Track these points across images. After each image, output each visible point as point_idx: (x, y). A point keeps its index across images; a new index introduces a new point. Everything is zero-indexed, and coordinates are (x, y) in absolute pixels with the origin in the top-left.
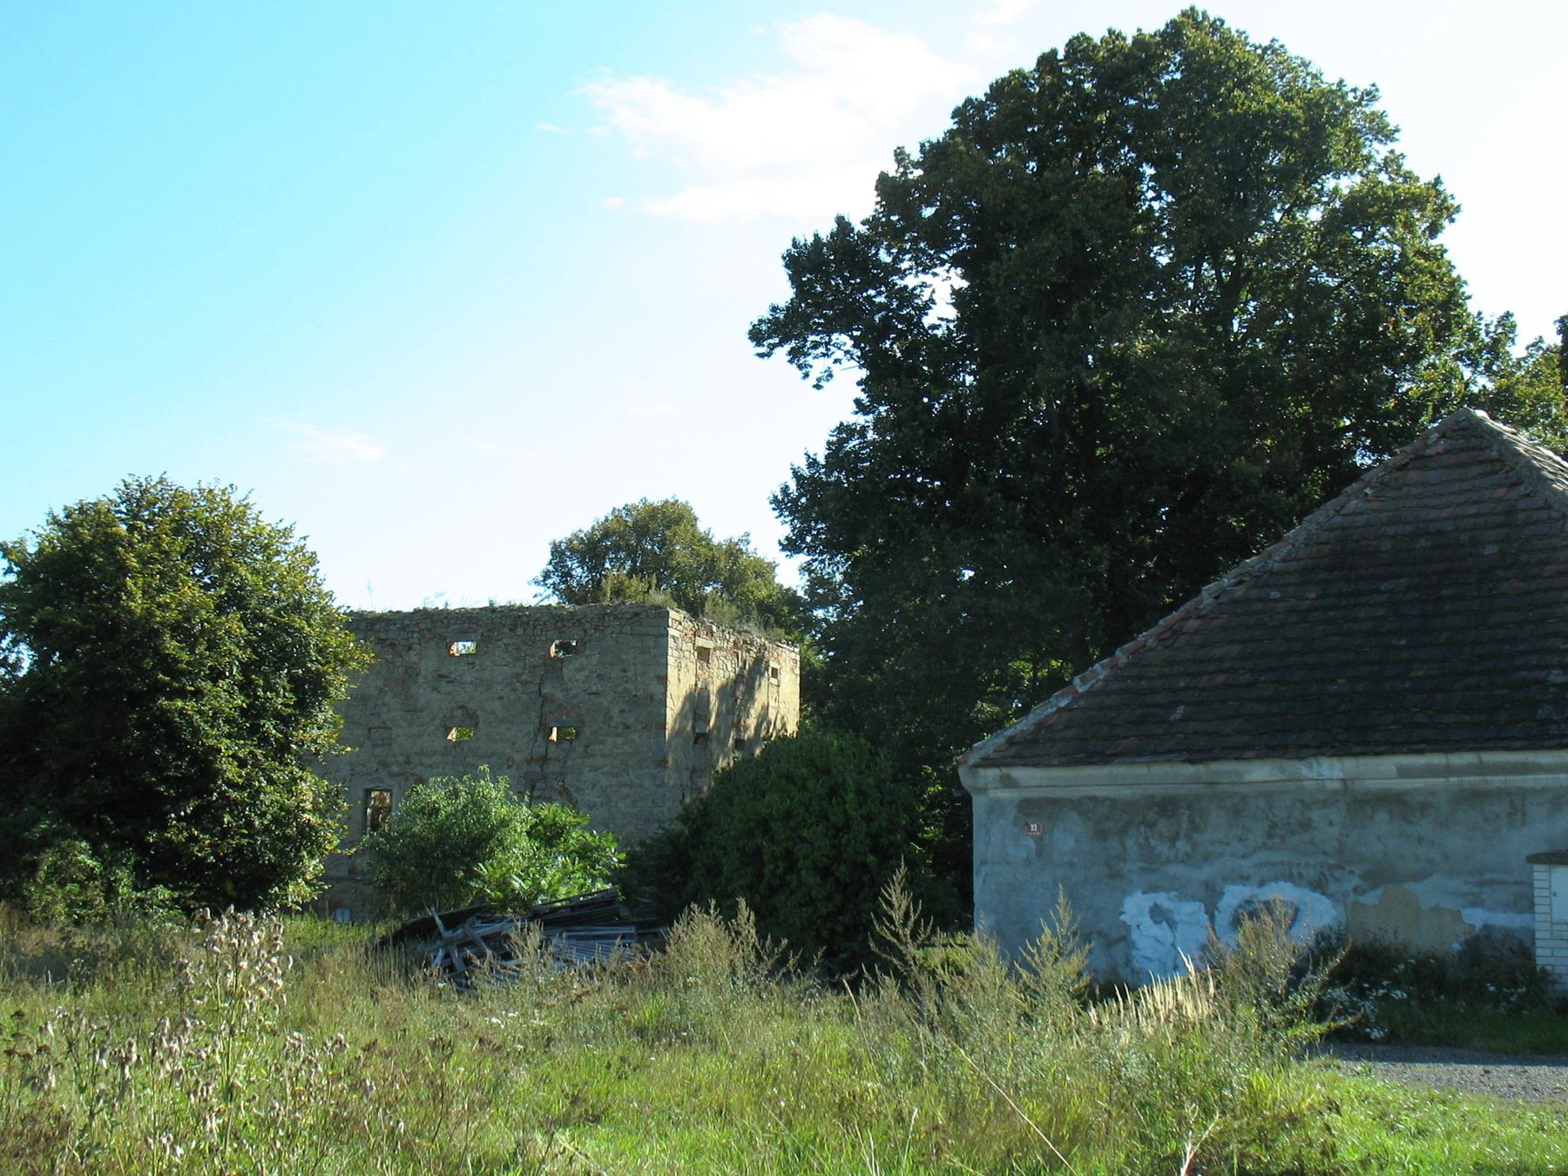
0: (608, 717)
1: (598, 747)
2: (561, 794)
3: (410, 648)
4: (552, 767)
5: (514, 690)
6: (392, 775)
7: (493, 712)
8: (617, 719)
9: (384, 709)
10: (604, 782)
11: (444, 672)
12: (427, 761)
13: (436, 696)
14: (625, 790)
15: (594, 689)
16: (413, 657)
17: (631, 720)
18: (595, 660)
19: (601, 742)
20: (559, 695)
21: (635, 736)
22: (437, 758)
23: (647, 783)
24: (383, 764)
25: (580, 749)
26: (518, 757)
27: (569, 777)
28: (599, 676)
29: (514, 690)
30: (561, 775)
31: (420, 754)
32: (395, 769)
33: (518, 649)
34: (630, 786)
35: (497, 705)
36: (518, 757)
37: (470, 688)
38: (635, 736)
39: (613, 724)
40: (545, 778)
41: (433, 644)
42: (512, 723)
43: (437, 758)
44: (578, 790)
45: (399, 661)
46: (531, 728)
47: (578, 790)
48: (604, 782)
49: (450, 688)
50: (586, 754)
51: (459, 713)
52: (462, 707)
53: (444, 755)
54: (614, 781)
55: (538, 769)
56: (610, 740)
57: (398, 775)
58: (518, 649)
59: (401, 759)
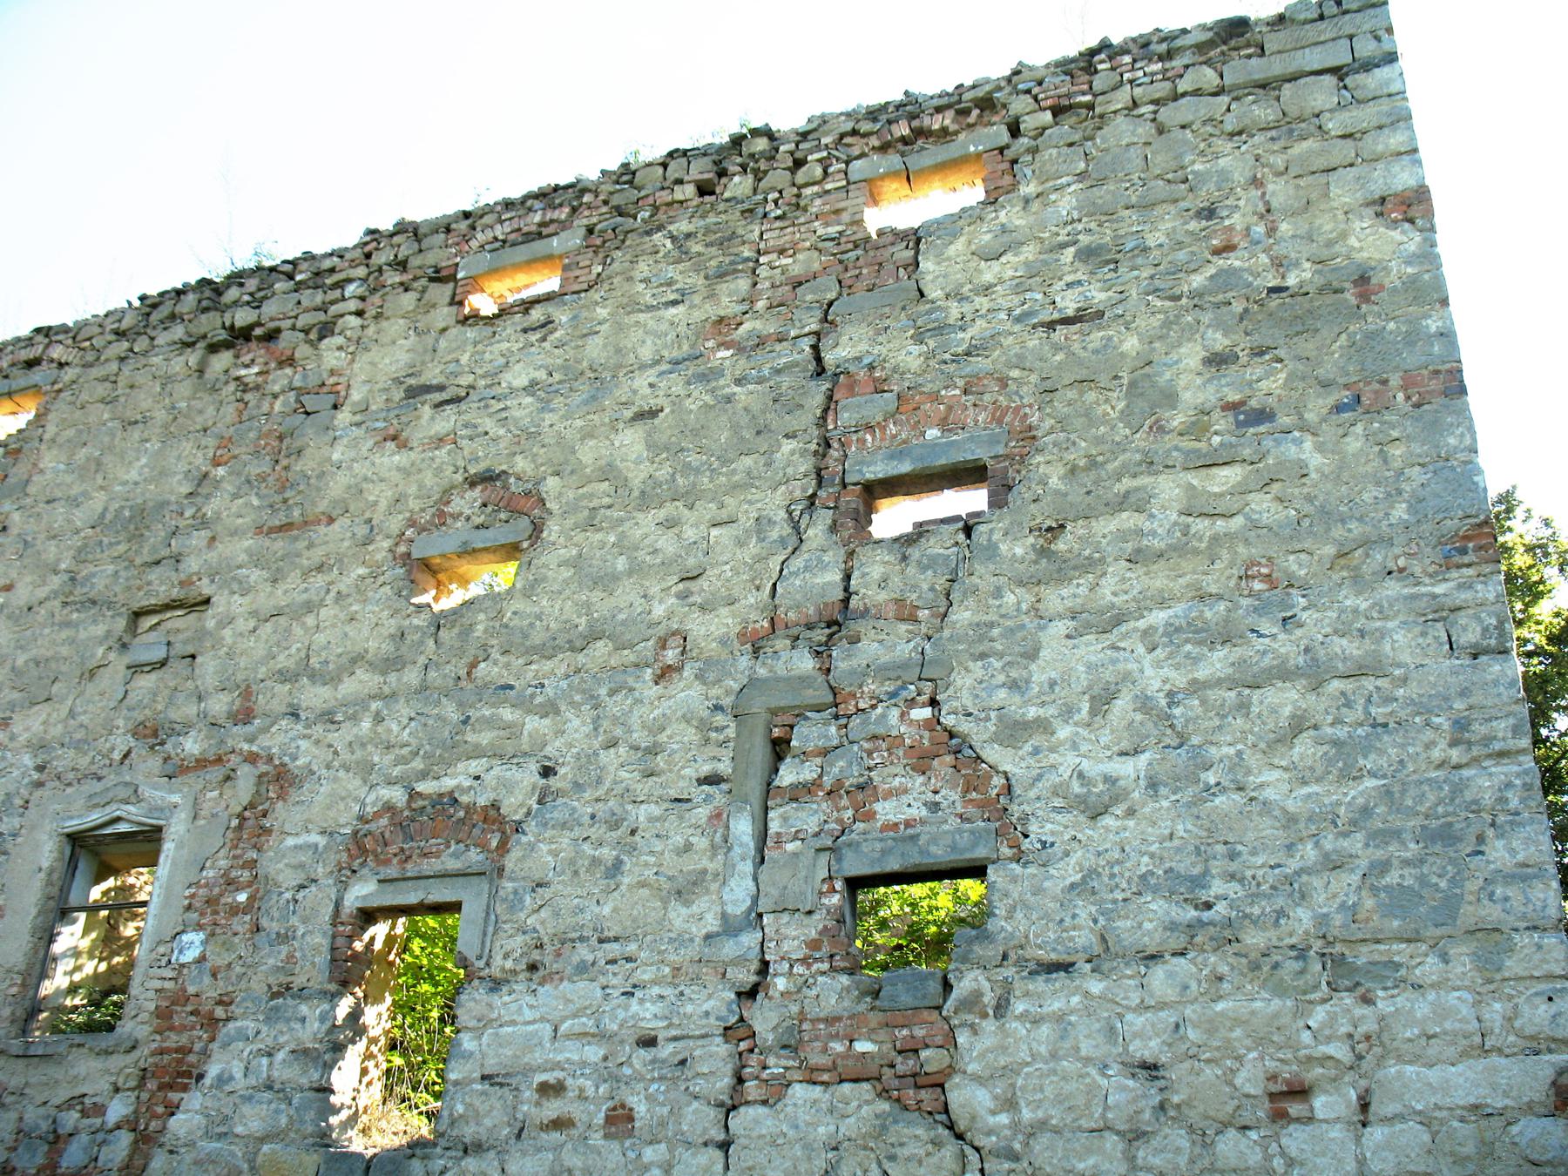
0: (1148, 395)
1: (1106, 526)
2: (921, 762)
3: (326, 330)
4: (878, 647)
6: (176, 771)
7: (608, 473)
8: (1195, 390)
9: (199, 538)
10: (1155, 675)
11: (432, 375)
12: (314, 696)
14: (1285, 699)
15: (1069, 304)
17: (1270, 384)
18: (1066, 204)
19: (1122, 503)
20: (908, 356)
21: (1307, 451)
23: (1401, 643)
25: (1020, 549)
28: (1087, 255)
30: (926, 681)
31: (285, 676)
32: (192, 745)
34: (1315, 673)
35: (631, 440)
36: (711, 629)
37: (523, 409)
38: (1307, 451)
39: (1177, 420)
40: (836, 704)
42: (690, 498)
44: (1013, 731)
45: (280, 379)
46: (774, 503)
47: (1013, 731)
48: (1155, 675)
49: (446, 421)
51: (467, 503)
52: (487, 478)
54: (1217, 662)
55: (805, 663)
56: (1168, 489)
57: (202, 763)
59: (219, 705)
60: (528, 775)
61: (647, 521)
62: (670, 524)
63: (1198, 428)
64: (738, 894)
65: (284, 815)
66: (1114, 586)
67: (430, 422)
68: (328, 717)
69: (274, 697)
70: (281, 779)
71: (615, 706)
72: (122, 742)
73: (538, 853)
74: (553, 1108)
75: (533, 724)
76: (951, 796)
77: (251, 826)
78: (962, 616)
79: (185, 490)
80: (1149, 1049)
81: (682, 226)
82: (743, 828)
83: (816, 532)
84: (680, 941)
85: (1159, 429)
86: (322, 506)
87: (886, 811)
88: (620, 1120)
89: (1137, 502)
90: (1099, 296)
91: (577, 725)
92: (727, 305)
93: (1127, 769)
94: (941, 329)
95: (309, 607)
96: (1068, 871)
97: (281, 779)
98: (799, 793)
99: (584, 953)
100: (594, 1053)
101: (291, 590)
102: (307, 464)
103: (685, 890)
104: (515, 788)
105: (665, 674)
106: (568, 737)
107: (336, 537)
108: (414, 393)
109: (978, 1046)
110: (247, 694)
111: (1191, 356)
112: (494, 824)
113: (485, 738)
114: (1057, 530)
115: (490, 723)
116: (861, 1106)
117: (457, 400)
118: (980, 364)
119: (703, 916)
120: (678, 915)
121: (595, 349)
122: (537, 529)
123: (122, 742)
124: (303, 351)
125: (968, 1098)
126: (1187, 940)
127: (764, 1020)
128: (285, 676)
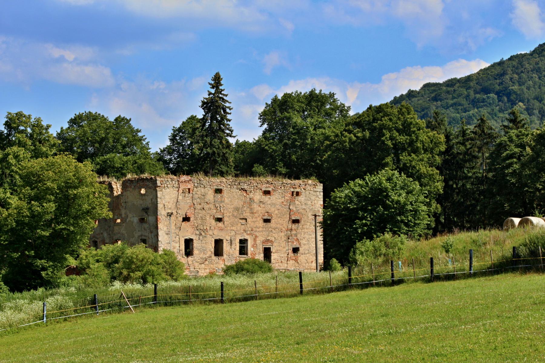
2: (296, 241)
5: (282, 207)
12: (258, 230)
16: (251, 195)
20: (295, 209)
22: (261, 229)
24: (245, 231)
26: (284, 229)
29: (282, 207)
30: (296, 235)
32: (249, 232)
40: (292, 235)
41: (258, 191)
43: (261, 229)
44: (301, 239)
47: (301, 239)
50: (303, 228)
52: (268, 212)
53: (263, 228)
54: (310, 237)
59: (250, 229)
65: (257, 239)
66: (306, 230)
67: (261, 205)
69: (254, 229)
70: (256, 237)
73: (275, 244)
77: (255, 240)
81: (279, 191)
87: (295, 244)
97: (256, 237)
101: (254, 219)
102: (252, 207)
104: (273, 239)
107: (256, 215)
108: (260, 202)
109: (299, 258)
111: (310, 214)
112: (271, 242)
116: (294, 262)
121: (274, 202)
126: (308, 253)
127: (289, 256)
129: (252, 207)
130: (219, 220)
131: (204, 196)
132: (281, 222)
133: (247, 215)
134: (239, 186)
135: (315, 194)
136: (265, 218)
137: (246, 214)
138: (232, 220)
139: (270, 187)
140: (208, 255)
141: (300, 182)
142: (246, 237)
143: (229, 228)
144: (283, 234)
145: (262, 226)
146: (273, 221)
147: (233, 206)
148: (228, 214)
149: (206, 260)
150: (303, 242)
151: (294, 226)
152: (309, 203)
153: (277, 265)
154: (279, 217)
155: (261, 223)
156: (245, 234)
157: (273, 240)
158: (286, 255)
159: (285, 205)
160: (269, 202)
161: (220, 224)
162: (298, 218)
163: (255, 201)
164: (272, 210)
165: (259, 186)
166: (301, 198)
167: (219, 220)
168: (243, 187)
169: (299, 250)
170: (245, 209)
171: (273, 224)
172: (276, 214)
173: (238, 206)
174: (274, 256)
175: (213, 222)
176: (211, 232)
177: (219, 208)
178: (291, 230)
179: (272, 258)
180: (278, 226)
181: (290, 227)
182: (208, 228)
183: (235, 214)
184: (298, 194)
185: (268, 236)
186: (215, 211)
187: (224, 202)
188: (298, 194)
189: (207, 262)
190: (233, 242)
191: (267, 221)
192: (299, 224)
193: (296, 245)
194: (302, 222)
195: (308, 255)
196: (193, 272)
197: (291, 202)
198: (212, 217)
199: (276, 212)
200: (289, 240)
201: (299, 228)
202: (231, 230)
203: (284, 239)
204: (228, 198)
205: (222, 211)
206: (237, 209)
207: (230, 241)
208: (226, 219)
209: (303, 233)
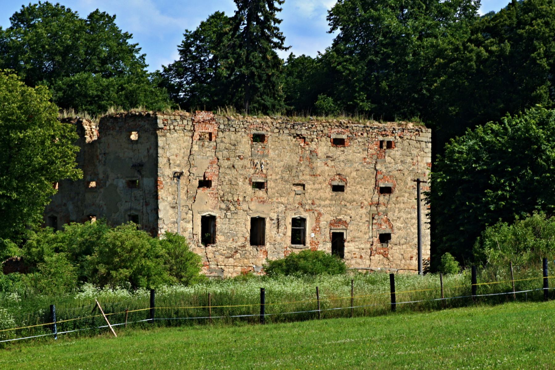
1: (402, 198)
2: (386, 222)
3: (312, 141)
4: (382, 208)
5: (364, 166)
6: (306, 210)
11: (330, 155)
12: (323, 203)
13: (327, 168)
16: (313, 146)
20: (384, 170)
22: (327, 202)
24: (301, 204)
25: (394, 199)
26: (366, 203)
27: (389, 214)
31: (318, 199)
32: (307, 207)
33: (364, 144)
37: (342, 165)
40: (378, 214)
41: (324, 139)
43: (327, 202)
44: (393, 220)
47: (393, 220)
50: (397, 202)
52: (339, 175)
53: (331, 200)
54: (409, 216)
56: (407, 195)
58: (364, 144)
59: (310, 202)
60: (349, 217)
61: (359, 186)
62: (361, 187)
63: (409, 188)
64: (371, 234)
65: (321, 219)
66: (402, 206)
68: (324, 206)
70: (320, 214)
71: (357, 210)
72: (297, 206)
73: (351, 227)
74: (355, 256)
75: (349, 211)
76: (388, 226)
77: (318, 220)
78: (389, 206)
79: (297, 164)
80: (402, 253)
81: (360, 140)
82: (371, 227)
83: (376, 192)
84: (366, 238)
85: (406, 187)
86: (318, 173)
87: (383, 227)
88: (361, 257)
89: (403, 196)
90: (402, 168)
91: (353, 212)
92: (365, 156)
93: (402, 226)
94: (388, 167)
95: (319, 189)
96: (396, 236)
97: (320, 214)
98: (375, 224)
99: (356, 239)
100: (358, 250)
101: (317, 186)
102: (314, 165)
103: (365, 233)
104: (348, 219)
105: (362, 207)
106: (352, 213)
107: (321, 179)
108: (328, 157)
109: (391, 251)
110: (313, 201)
111: (409, 179)
113: (344, 212)
114: (397, 197)
115: (344, 210)
116: (382, 257)
117: (333, 160)
118: (391, 174)
119: (367, 237)
120: (365, 236)
121: (350, 157)
122: (346, 184)
123: (297, 206)
124: (310, 143)
125: (389, 256)
126: (405, 243)
127: (374, 248)
128: (318, 199)
129: (314, 165)
130: (259, 186)
131: (234, 145)
132: (361, 191)
133: (305, 178)
134: (293, 131)
135: (418, 145)
136: (335, 183)
137: (304, 177)
138: (280, 186)
139: (344, 133)
140: (239, 244)
141: (395, 125)
142: (304, 215)
143: (275, 199)
144: (364, 211)
145: (330, 198)
146: (347, 189)
147: (282, 163)
148: (274, 177)
149: (236, 252)
150: (397, 224)
151: (383, 199)
152: (409, 160)
153: (353, 262)
154: (358, 183)
155: (328, 193)
156: (301, 209)
157: (348, 221)
158: (369, 246)
159: (368, 163)
160: (342, 158)
161: (261, 193)
162: (389, 185)
163: (320, 155)
164: (347, 170)
165: (326, 131)
166: (396, 152)
167: (259, 186)
168: (299, 133)
169: (390, 238)
170: (302, 168)
171: (348, 194)
172: (354, 178)
173: (291, 163)
174: (348, 247)
175: (249, 189)
176: (245, 206)
177: (259, 166)
178: (378, 204)
179: (346, 250)
180: (356, 197)
181: (376, 199)
182: (241, 199)
183: (286, 176)
184: (390, 145)
185: (340, 214)
186: (252, 171)
187: (267, 156)
188: (390, 145)
189: (238, 255)
190: (282, 222)
191: (338, 189)
192: (392, 195)
193: (385, 229)
194: (396, 192)
195: (404, 247)
196: (216, 271)
197: (379, 157)
198: (247, 181)
199: (354, 174)
200: (375, 221)
201: (391, 202)
202: (279, 203)
203: (365, 219)
204: (274, 150)
205: (264, 171)
206: (289, 168)
207: (276, 221)
208: (270, 184)
209: (397, 210)
